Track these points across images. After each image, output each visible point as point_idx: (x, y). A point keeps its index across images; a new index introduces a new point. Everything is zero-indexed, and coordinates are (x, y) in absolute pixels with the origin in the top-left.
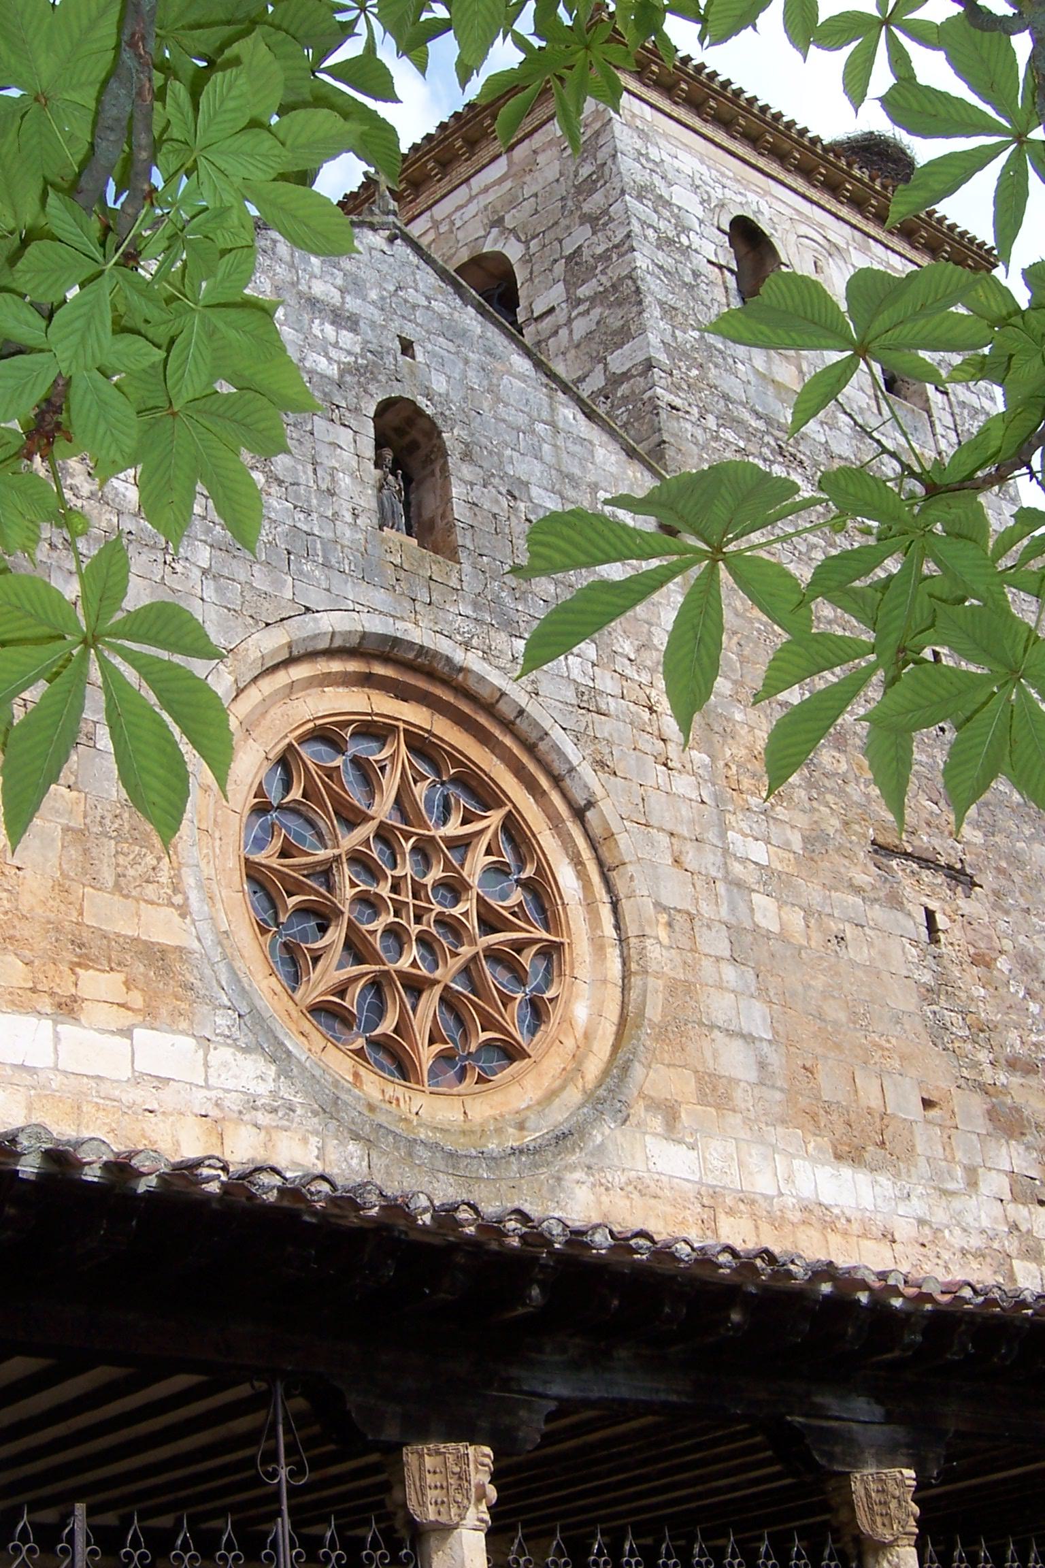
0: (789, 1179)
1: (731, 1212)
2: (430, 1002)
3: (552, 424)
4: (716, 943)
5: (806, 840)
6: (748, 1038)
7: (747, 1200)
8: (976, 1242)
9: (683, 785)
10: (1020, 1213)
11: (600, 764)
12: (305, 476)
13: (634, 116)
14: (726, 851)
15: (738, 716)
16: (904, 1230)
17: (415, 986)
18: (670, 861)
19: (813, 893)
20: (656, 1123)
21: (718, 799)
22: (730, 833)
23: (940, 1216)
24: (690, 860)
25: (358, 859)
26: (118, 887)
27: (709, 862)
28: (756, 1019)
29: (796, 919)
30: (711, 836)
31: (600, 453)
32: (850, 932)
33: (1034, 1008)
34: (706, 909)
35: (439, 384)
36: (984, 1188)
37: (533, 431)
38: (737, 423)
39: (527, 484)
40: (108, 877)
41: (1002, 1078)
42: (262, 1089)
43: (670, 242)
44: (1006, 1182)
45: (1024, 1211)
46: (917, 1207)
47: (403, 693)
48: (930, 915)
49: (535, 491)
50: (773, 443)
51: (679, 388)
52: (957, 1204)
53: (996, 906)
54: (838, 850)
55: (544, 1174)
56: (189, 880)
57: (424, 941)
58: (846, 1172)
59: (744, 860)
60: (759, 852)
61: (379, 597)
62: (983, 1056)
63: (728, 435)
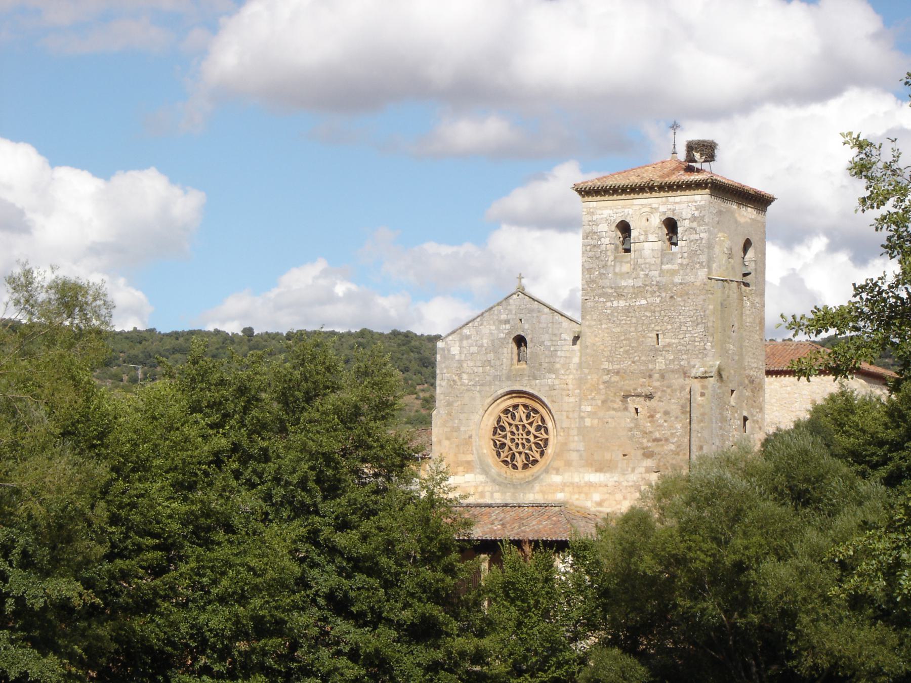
0: (583, 478)
1: (568, 486)
2: (523, 456)
3: (553, 323)
4: (575, 432)
5: (603, 402)
6: (578, 451)
7: (572, 484)
8: (630, 484)
9: (572, 399)
10: (647, 476)
11: (553, 401)
12: (498, 363)
13: (590, 208)
14: (580, 411)
15: (589, 377)
16: (610, 484)
17: (520, 453)
18: (565, 417)
19: (601, 414)
20: (554, 472)
21: (580, 400)
22: (582, 407)
23: (622, 480)
24: (571, 416)
25: (513, 433)
26: (463, 453)
27: (576, 415)
28: (581, 446)
29: (596, 421)
30: (577, 409)
31: (564, 323)
32: (610, 420)
33: (665, 424)
34: (573, 426)
35: (527, 326)
36: (636, 472)
37: (547, 327)
38: (604, 295)
39: (544, 342)
40: (462, 451)
41: (650, 444)
42: (483, 480)
43: (595, 246)
44: (644, 469)
45: (648, 475)
46: (616, 479)
47: (520, 397)
48: (636, 409)
49: (545, 343)
50: (615, 294)
51: (588, 293)
52: (627, 476)
53: (659, 401)
54: (612, 401)
55: (531, 485)
56: (474, 448)
57: (523, 444)
58: (598, 474)
59: (584, 412)
60: (589, 409)
61: (509, 383)
62: (645, 441)
63: (602, 299)
